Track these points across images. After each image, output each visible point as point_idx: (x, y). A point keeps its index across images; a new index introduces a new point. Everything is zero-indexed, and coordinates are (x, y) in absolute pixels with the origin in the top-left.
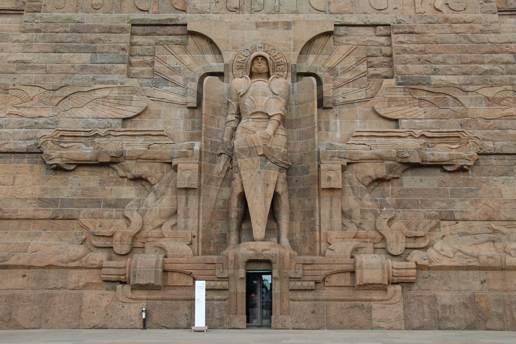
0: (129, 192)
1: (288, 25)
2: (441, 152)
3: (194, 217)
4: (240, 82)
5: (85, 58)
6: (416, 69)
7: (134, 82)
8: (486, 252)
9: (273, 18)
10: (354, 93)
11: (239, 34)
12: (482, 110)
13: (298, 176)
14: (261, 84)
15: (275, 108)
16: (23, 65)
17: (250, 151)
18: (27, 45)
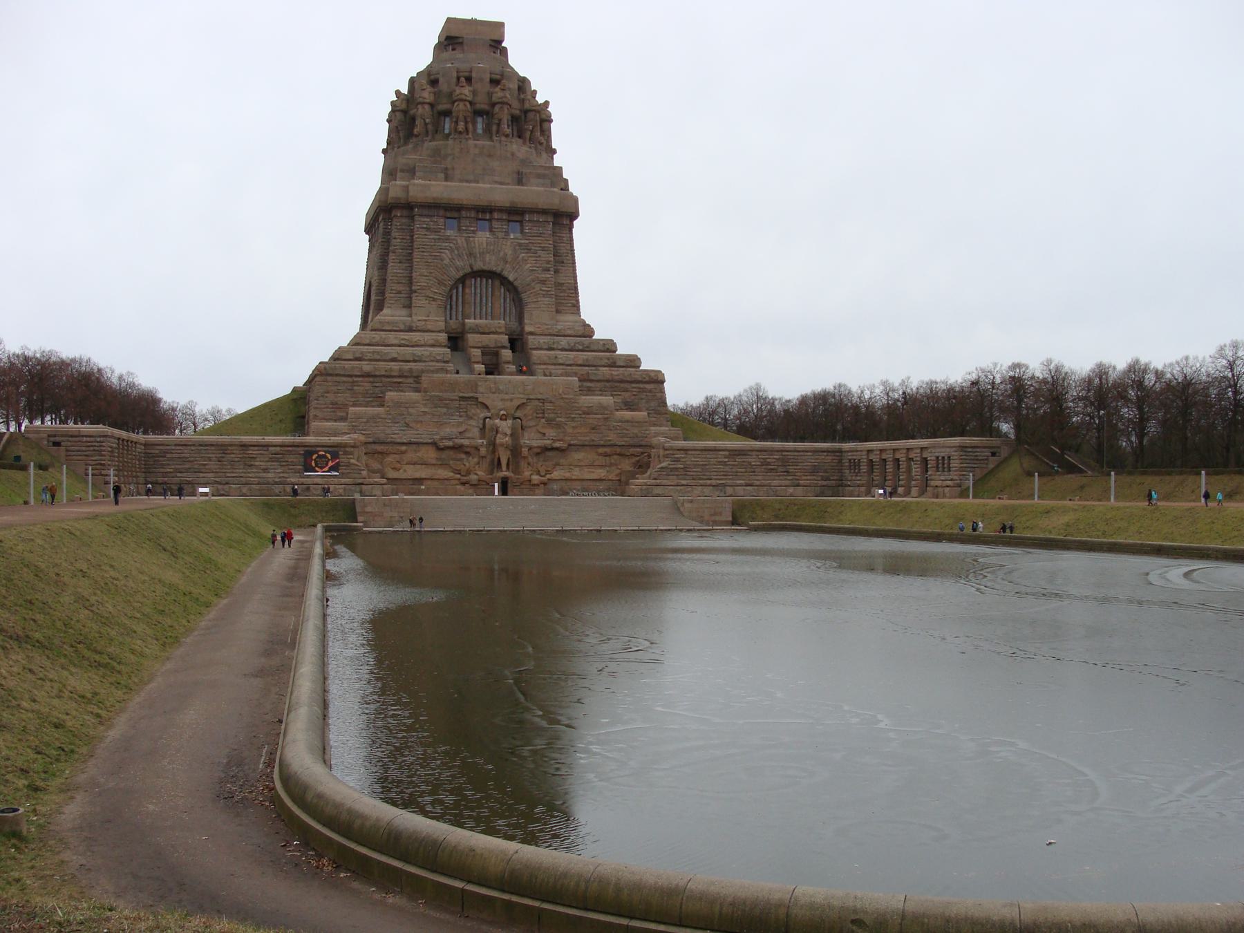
0: (463, 456)
1: (511, 400)
2: (557, 445)
3: (485, 464)
4: (497, 421)
5: (444, 410)
6: (552, 415)
7: (461, 420)
8: (568, 475)
9: (507, 397)
10: (532, 423)
11: (495, 402)
12: (570, 430)
13: (515, 451)
14: (504, 423)
15: (509, 432)
16: (425, 413)
17: (502, 445)
18: (425, 405)
